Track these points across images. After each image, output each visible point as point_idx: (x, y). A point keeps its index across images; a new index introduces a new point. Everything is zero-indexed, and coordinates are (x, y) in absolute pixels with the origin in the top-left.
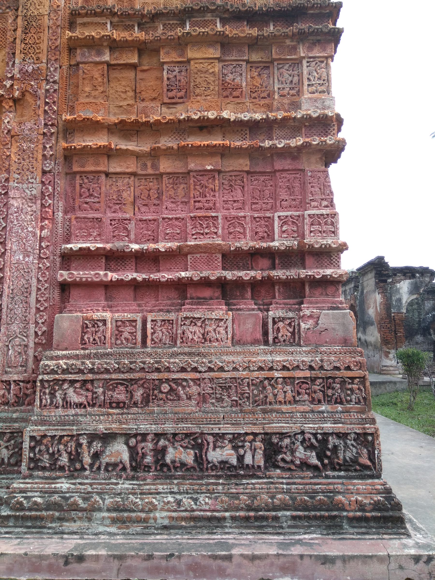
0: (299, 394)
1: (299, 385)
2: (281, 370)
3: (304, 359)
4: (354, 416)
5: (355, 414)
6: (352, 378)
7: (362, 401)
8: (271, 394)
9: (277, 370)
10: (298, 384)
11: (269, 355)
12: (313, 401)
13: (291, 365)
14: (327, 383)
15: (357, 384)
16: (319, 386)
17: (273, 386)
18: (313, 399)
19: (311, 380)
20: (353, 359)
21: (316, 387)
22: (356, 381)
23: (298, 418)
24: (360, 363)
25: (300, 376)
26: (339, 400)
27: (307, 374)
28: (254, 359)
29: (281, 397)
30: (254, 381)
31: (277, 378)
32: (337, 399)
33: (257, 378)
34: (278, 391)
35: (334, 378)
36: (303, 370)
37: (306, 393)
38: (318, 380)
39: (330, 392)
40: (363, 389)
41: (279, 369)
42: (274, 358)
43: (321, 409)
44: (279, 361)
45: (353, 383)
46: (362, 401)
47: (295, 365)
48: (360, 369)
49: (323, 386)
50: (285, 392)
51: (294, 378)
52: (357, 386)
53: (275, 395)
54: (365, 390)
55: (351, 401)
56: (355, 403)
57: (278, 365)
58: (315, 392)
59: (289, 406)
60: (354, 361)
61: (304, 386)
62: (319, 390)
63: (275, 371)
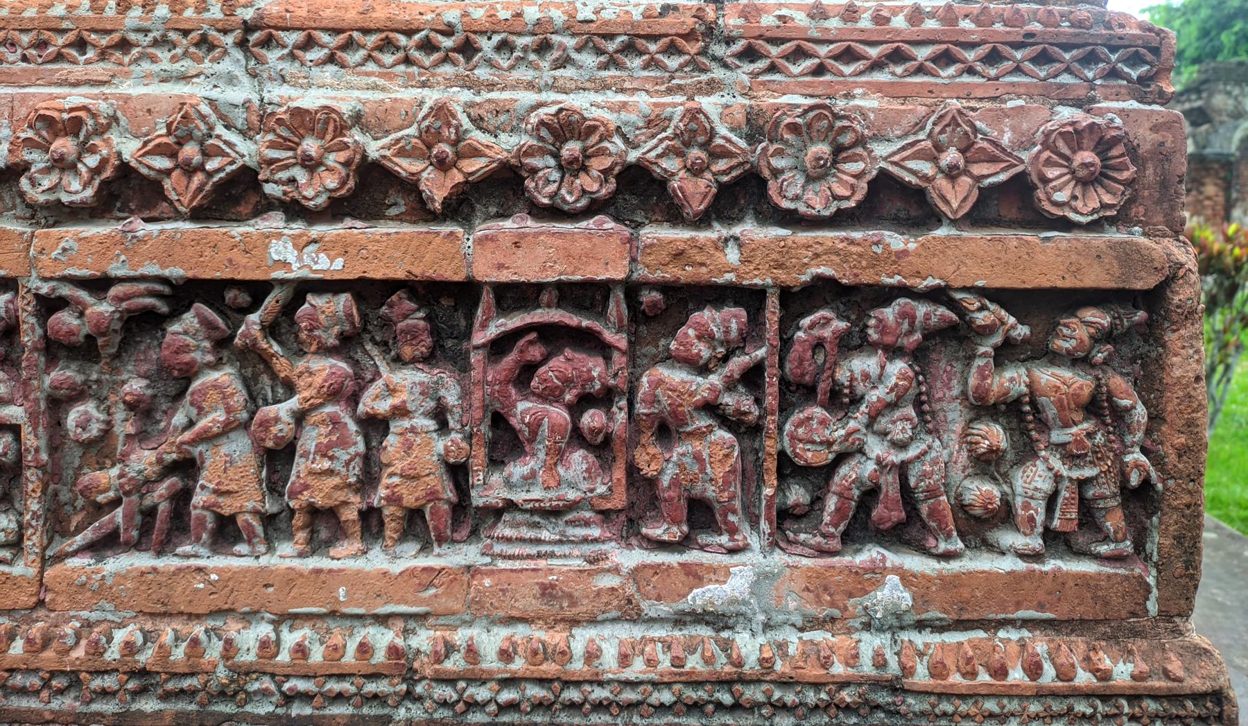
0: (505, 441)
1: (510, 359)
2: (336, 209)
3: (578, 101)
4: (1034, 670)
5: (1041, 647)
6: (1044, 305)
7: (1114, 522)
8: (239, 447)
9: (295, 210)
10: (499, 347)
11: (233, 63)
12: (635, 509)
13: (442, 165)
14: (786, 343)
15: (1079, 360)
16: (704, 370)
17: (253, 363)
18: (643, 489)
19: (638, 317)
20: (1066, 113)
21: (677, 376)
22: (1076, 331)
23: (480, 680)
24: (1132, 151)
25: (527, 268)
26: (887, 512)
27: (597, 250)
28: (76, 97)
29: (319, 474)
30: (66, 319)
31: (303, 288)
32: (871, 494)
33: (99, 285)
34: (300, 417)
35: (857, 299)
36: (555, 212)
37: (578, 437)
38: (708, 316)
39: (811, 431)
40: (1140, 413)
41: (314, 190)
42: (276, 92)
43: (699, 597)
44: (327, 123)
45: (1038, 351)
46: (1114, 522)
47: (474, 166)
48: (1121, 218)
49: (752, 378)
50: (375, 426)
51: (465, 293)
52: (1078, 382)
53: (278, 457)
54: (1156, 418)
55: (1005, 515)
56: (1049, 535)
57: (311, 165)
58: (666, 430)
59: (409, 558)
60: (1075, 137)
61: (559, 365)
62: (711, 408)
63: (274, 221)
